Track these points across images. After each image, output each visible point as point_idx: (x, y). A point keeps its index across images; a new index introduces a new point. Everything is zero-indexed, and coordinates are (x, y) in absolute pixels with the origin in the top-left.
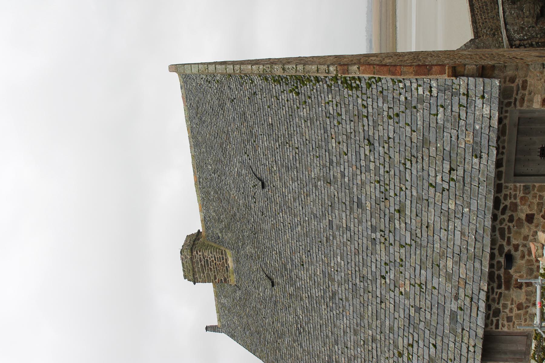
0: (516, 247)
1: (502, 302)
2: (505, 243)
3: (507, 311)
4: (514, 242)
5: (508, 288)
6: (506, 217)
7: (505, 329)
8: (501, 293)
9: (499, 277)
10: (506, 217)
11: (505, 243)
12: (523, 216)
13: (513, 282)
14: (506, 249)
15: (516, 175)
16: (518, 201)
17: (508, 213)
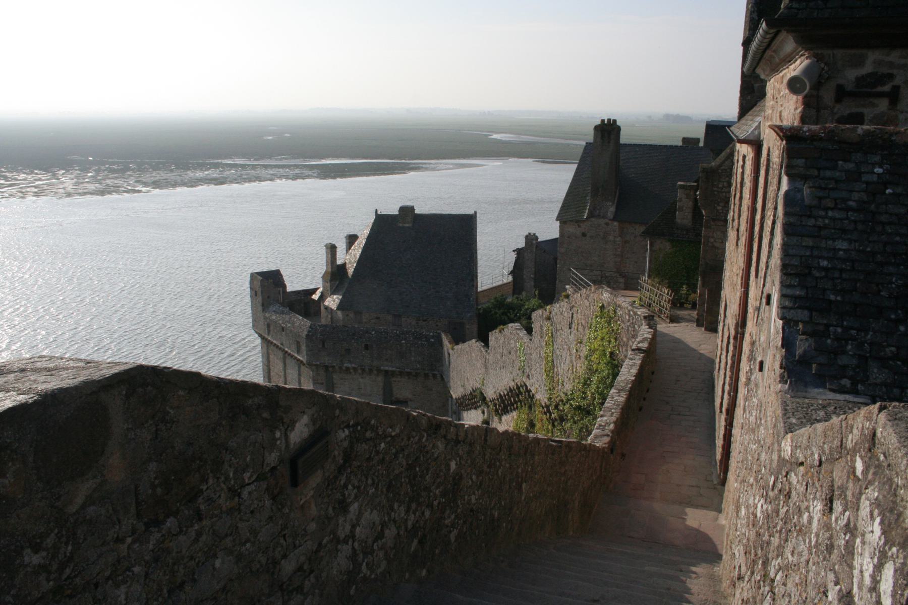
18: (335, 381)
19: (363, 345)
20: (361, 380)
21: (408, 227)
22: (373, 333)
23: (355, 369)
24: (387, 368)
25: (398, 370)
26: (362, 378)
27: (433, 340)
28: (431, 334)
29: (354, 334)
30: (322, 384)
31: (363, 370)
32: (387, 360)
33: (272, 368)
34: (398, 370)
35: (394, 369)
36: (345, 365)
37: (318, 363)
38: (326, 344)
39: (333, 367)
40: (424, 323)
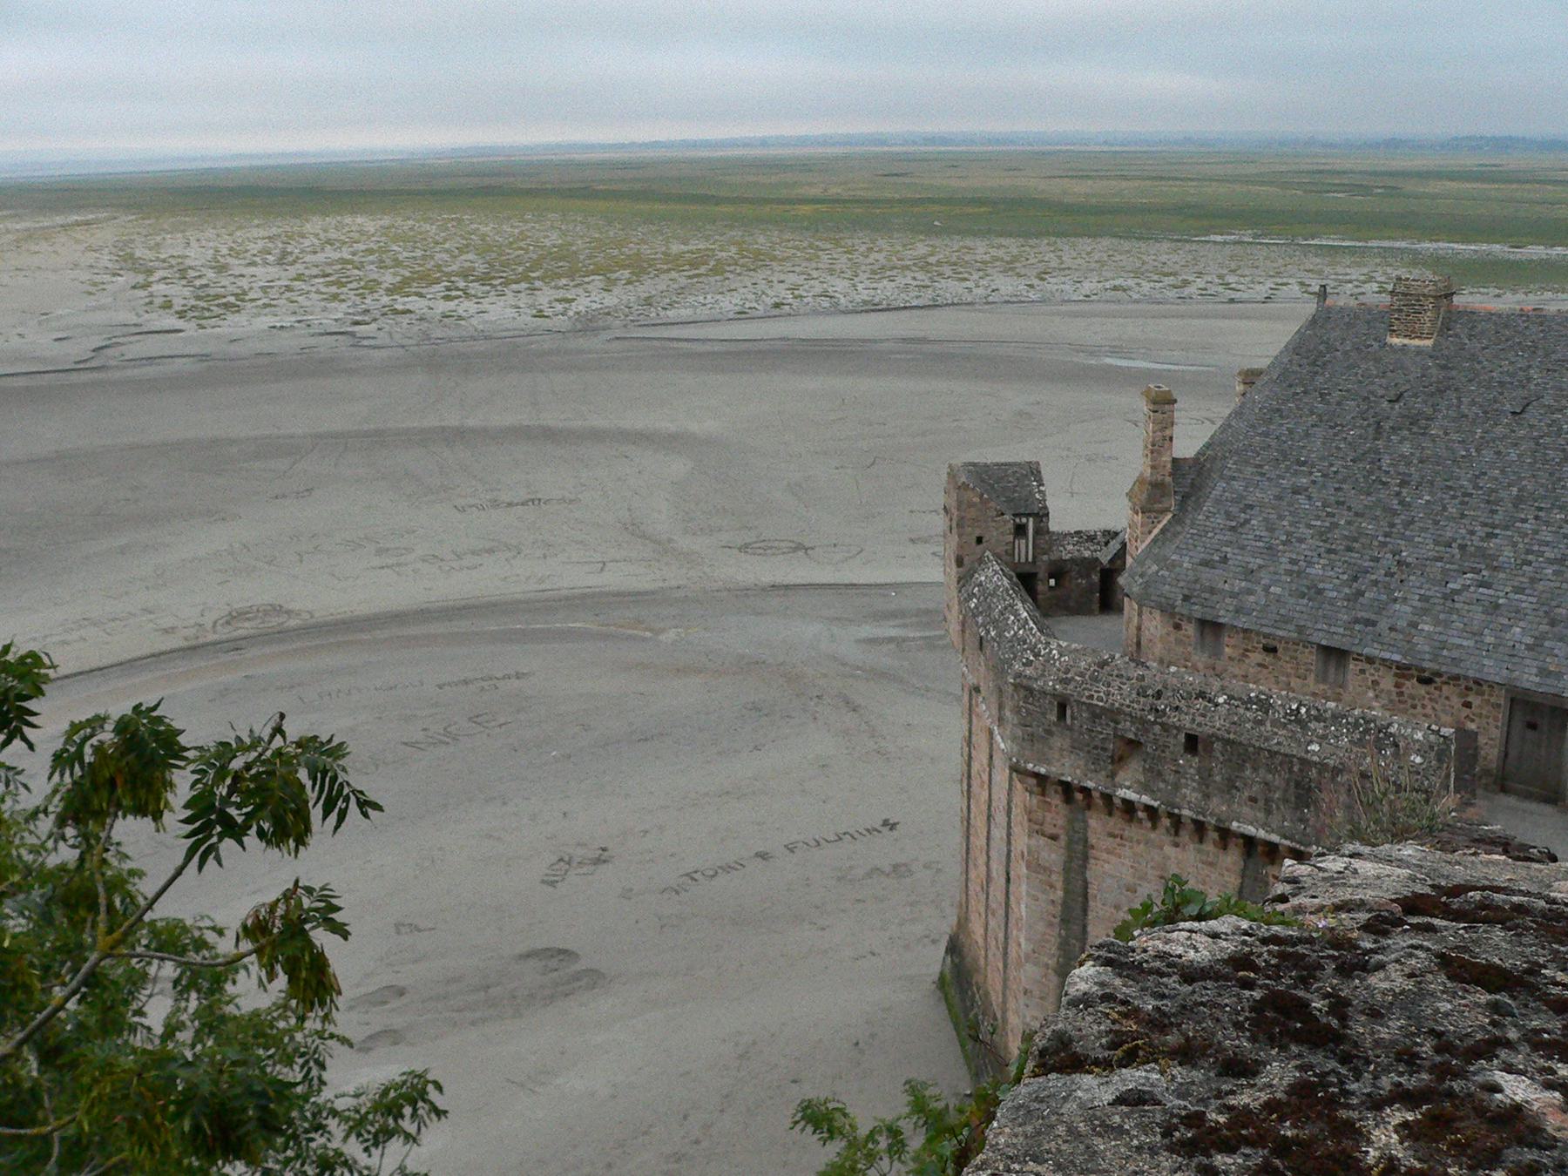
0: (1439, 689)
1: (1382, 668)
2: (1443, 679)
3: (1373, 671)
4: (1445, 688)
5: (1396, 675)
6: (1471, 684)
7: (1351, 666)
8: (1391, 668)
9: (1409, 669)
10: (1471, 684)
11: (1443, 679)
12: (1470, 699)
13: (1402, 680)
14: (1437, 679)
15: (1512, 700)
16: (1486, 697)
17: (1475, 687)
18: (1093, 840)
19: (1182, 738)
20: (1169, 850)
21: (1419, 351)
22: (1221, 700)
23: (1152, 812)
24: (1250, 830)
25: (1287, 843)
26: (1176, 845)
27: (1418, 760)
28: (1419, 736)
29: (1159, 695)
30: (1054, 838)
31: (1177, 822)
32: (1253, 800)
33: (973, 752)
34: (1287, 843)
35: (1275, 838)
36: (1121, 793)
37: (1043, 771)
38: (1068, 712)
39: (1086, 791)
40: (1422, 690)
